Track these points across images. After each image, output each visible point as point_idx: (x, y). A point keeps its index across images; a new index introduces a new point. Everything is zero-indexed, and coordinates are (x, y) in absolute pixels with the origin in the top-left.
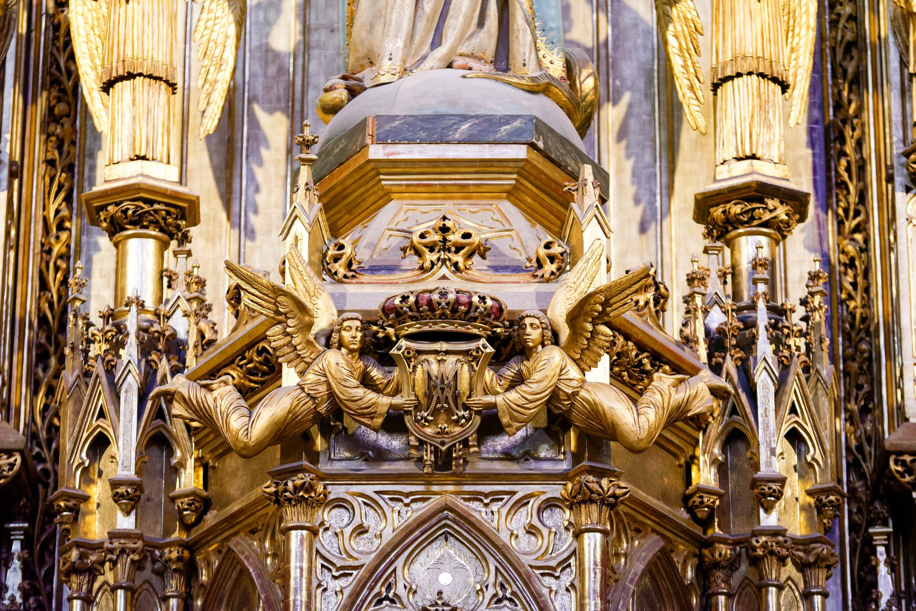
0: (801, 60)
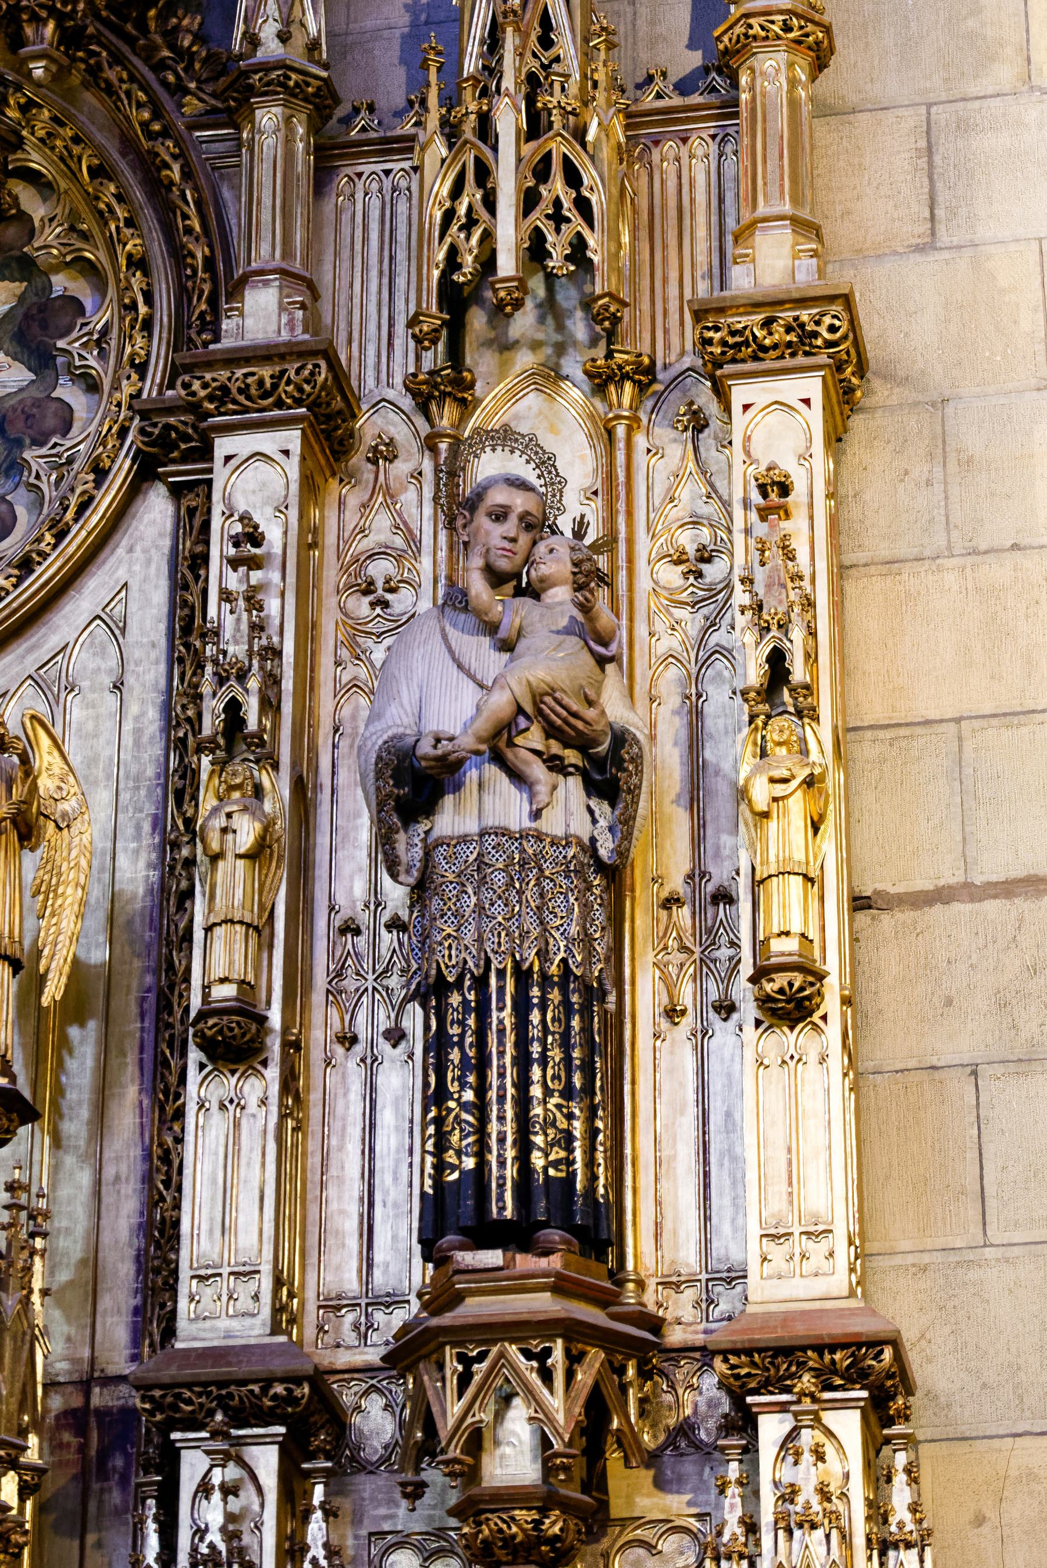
0: (64, 924)
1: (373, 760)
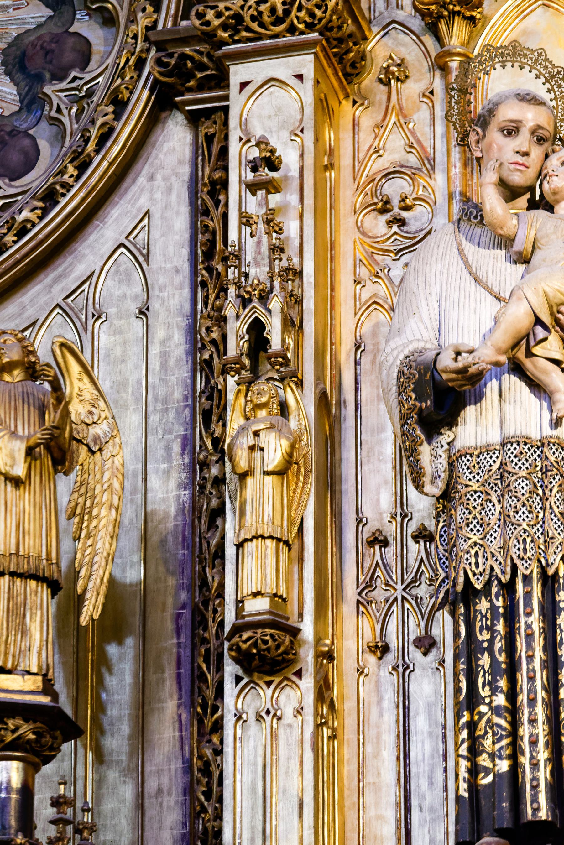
0: (99, 545)
1: (395, 375)
